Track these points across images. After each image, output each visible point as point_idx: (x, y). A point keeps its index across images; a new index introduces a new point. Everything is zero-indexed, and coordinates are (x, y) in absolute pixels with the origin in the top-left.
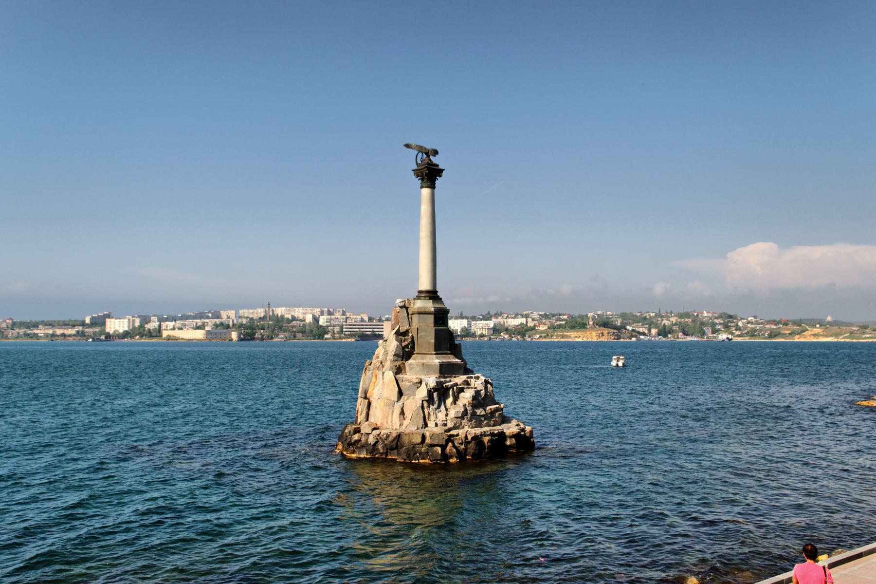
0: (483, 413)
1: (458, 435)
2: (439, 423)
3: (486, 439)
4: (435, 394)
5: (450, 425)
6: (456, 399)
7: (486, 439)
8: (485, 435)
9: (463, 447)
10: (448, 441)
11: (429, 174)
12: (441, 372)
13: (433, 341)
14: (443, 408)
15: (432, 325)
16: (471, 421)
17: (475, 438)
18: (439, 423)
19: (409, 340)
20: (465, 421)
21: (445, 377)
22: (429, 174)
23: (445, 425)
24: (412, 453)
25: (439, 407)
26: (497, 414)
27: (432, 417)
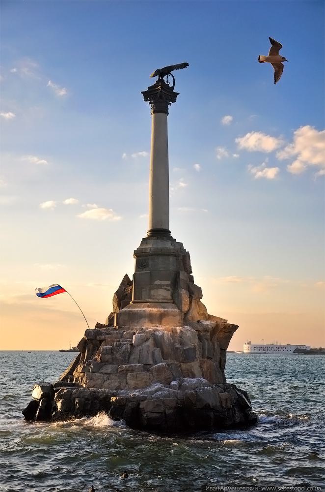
0: (109, 371)
11: (160, 97)
22: (160, 97)
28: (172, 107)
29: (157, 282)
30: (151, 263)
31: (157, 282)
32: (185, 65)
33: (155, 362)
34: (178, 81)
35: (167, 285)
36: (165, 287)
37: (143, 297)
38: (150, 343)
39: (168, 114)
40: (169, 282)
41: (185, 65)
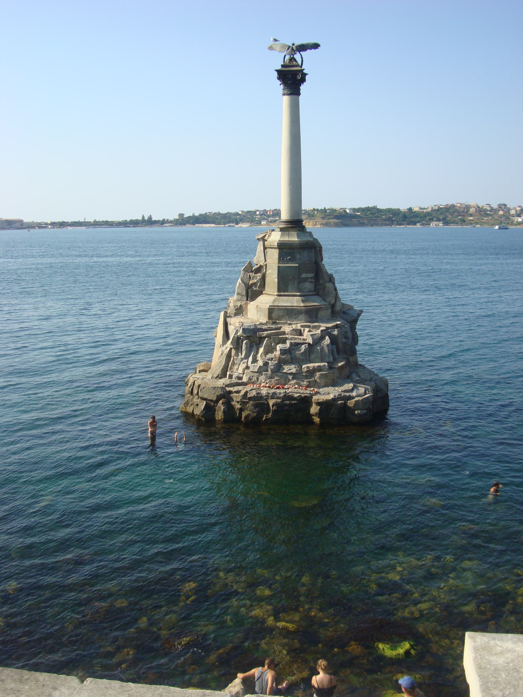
0: (294, 371)
1: (238, 392)
2: (235, 375)
3: (271, 402)
4: (245, 342)
5: (245, 379)
6: (269, 350)
7: (271, 402)
8: (272, 398)
9: (238, 406)
10: (219, 398)
12: (270, 317)
13: (276, 280)
14: (250, 359)
15: (277, 261)
16: (271, 377)
17: (258, 397)
18: (235, 375)
19: (258, 278)
20: (262, 378)
21: (274, 323)
22: (292, 79)
23: (241, 378)
24: (191, 403)
25: (247, 357)
26: (318, 374)
27: (236, 367)
28: (303, 88)
29: (304, 276)
30: (298, 256)
31: (304, 276)
32: (316, 46)
33: (335, 361)
34: (308, 61)
35: (311, 278)
36: (310, 280)
37: (289, 290)
38: (327, 340)
39: (299, 94)
40: (312, 275)
41: (316, 46)
